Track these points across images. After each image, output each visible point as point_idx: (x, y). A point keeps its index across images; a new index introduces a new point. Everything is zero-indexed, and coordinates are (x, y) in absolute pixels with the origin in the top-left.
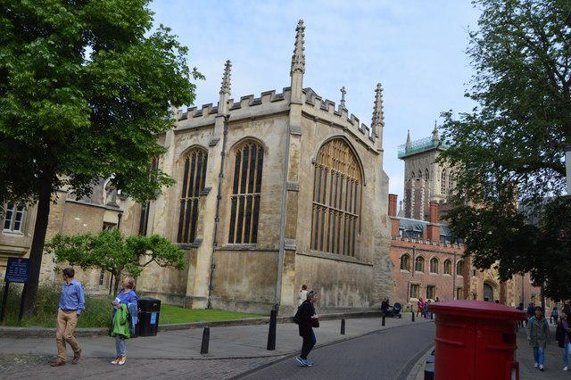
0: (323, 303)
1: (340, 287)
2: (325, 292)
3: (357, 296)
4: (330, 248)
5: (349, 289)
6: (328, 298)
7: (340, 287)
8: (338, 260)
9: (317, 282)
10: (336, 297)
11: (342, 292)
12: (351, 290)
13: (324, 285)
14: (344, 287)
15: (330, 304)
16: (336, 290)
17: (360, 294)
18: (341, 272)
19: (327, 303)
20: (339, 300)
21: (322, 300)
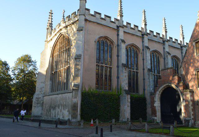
0: (52, 116)
1: (59, 108)
2: (53, 111)
3: (67, 112)
4: (59, 89)
5: (62, 107)
6: (54, 114)
7: (59, 108)
8: (58, 94)
9: (50, 106)
10: (57, 113)
11: (59, 110)
12: (64, 109)
13: (52, 108)
14: (60, 108)
15: (54, 116)
16: (57, 110)
17: (68, 111)
18: (59, 100)
19: (53, 116)
20: (58, 114)
21: (52, 114)
